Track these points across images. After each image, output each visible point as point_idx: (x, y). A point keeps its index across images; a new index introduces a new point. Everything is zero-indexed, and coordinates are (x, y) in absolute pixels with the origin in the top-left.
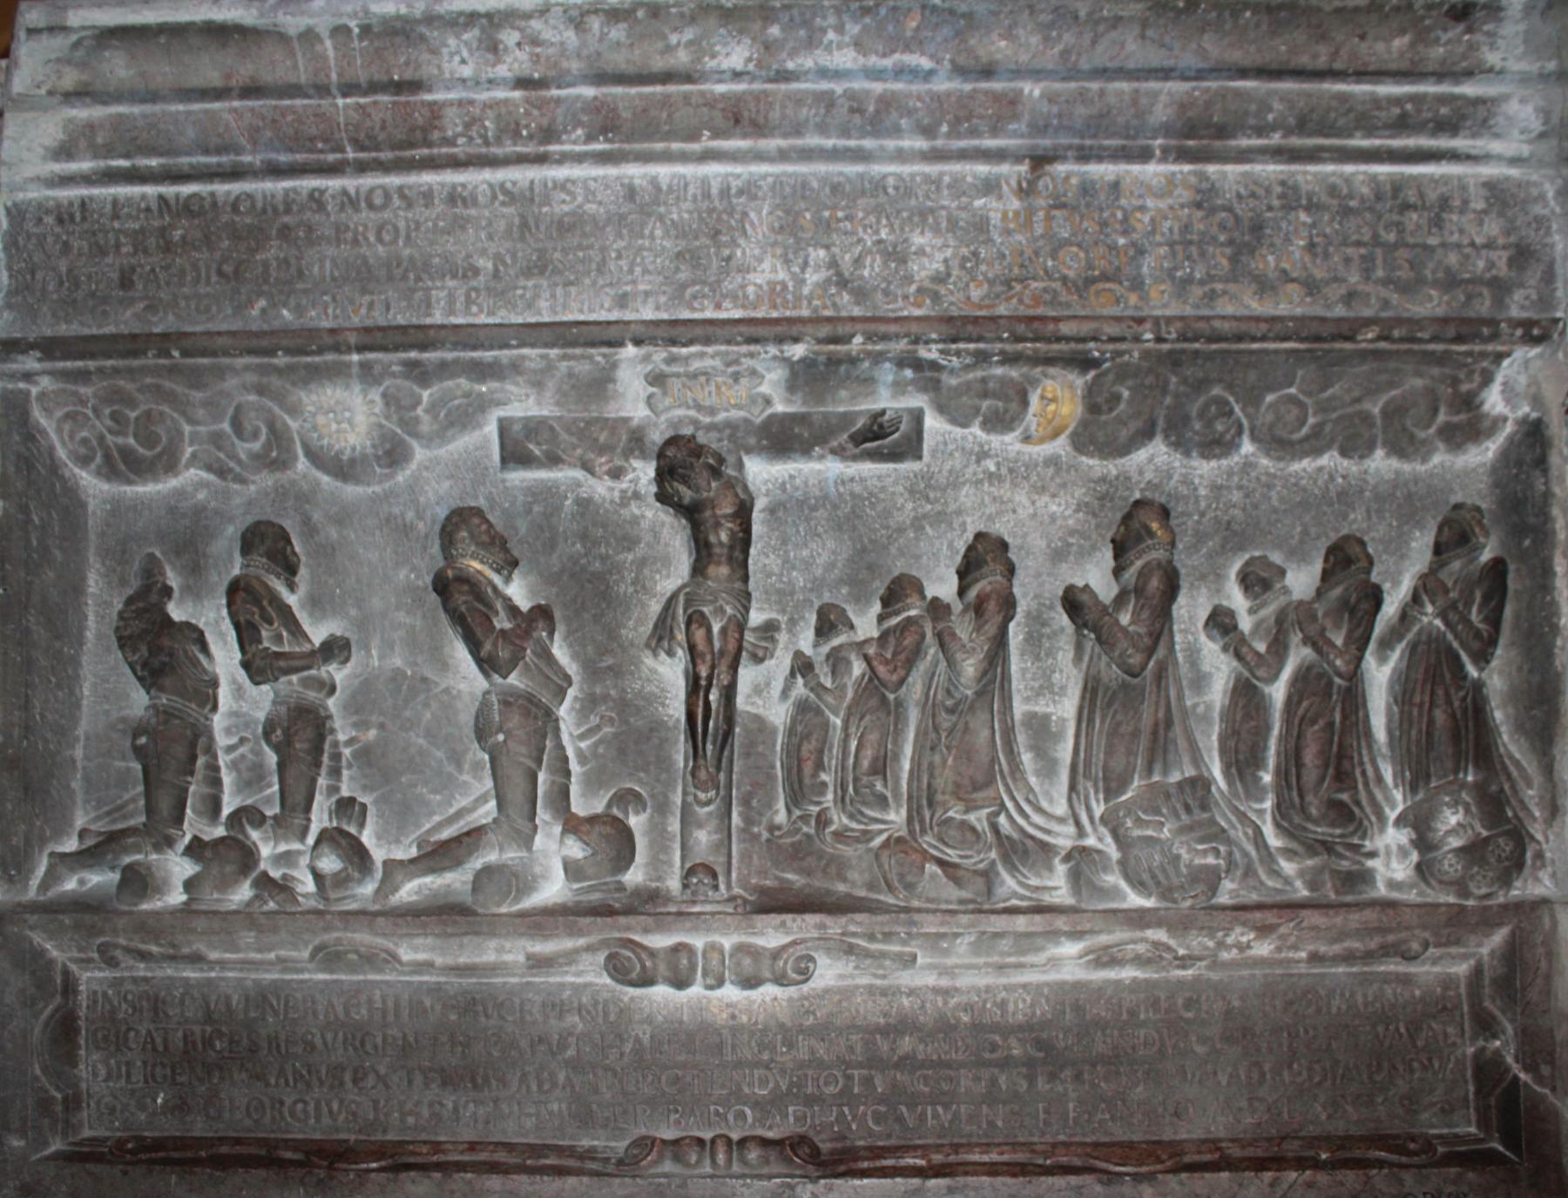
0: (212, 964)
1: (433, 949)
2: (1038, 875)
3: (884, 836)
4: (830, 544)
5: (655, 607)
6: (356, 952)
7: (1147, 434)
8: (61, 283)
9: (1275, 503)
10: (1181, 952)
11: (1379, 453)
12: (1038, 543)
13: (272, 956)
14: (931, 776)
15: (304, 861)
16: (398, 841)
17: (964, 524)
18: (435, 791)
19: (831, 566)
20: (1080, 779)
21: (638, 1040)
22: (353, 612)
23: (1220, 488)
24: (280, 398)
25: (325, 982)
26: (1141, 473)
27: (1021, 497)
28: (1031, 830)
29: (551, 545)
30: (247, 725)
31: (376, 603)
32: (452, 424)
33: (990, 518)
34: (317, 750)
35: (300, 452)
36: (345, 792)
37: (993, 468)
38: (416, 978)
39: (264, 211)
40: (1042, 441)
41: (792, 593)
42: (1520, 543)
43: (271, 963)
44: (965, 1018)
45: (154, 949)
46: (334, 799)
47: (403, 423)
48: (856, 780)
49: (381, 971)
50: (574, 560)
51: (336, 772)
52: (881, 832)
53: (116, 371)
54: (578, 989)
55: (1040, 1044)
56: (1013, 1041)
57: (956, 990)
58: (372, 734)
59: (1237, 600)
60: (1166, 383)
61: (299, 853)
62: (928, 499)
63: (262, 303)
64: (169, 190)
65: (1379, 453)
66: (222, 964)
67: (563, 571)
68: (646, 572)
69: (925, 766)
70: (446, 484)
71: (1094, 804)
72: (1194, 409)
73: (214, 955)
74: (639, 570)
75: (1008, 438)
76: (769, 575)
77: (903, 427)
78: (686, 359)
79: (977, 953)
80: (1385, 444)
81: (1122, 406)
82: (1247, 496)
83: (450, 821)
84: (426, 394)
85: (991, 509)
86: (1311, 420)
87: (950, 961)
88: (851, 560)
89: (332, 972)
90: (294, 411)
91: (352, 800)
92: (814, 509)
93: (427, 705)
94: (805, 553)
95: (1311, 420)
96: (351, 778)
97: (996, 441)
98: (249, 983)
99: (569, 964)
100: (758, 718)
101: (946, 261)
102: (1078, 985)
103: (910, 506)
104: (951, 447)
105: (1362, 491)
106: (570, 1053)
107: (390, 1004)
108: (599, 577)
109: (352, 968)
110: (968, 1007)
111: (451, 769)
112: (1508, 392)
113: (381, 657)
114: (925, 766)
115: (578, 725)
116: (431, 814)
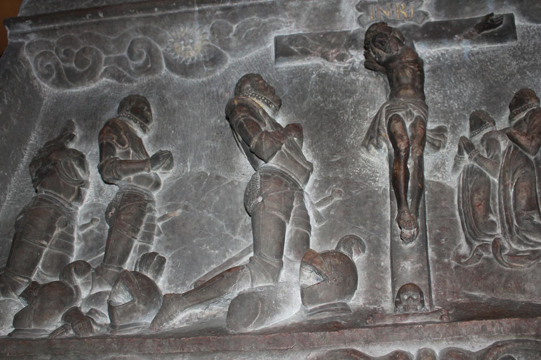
19: (473, 96)
22: (180, 142)
29: (303, 98)
50: (316, 104)
62: (524, 59)
68: (360, 107)
76: (436, 103)
77: (504, 22)
103: (515, 63)
104: (532, 34)
111: (228, 232)
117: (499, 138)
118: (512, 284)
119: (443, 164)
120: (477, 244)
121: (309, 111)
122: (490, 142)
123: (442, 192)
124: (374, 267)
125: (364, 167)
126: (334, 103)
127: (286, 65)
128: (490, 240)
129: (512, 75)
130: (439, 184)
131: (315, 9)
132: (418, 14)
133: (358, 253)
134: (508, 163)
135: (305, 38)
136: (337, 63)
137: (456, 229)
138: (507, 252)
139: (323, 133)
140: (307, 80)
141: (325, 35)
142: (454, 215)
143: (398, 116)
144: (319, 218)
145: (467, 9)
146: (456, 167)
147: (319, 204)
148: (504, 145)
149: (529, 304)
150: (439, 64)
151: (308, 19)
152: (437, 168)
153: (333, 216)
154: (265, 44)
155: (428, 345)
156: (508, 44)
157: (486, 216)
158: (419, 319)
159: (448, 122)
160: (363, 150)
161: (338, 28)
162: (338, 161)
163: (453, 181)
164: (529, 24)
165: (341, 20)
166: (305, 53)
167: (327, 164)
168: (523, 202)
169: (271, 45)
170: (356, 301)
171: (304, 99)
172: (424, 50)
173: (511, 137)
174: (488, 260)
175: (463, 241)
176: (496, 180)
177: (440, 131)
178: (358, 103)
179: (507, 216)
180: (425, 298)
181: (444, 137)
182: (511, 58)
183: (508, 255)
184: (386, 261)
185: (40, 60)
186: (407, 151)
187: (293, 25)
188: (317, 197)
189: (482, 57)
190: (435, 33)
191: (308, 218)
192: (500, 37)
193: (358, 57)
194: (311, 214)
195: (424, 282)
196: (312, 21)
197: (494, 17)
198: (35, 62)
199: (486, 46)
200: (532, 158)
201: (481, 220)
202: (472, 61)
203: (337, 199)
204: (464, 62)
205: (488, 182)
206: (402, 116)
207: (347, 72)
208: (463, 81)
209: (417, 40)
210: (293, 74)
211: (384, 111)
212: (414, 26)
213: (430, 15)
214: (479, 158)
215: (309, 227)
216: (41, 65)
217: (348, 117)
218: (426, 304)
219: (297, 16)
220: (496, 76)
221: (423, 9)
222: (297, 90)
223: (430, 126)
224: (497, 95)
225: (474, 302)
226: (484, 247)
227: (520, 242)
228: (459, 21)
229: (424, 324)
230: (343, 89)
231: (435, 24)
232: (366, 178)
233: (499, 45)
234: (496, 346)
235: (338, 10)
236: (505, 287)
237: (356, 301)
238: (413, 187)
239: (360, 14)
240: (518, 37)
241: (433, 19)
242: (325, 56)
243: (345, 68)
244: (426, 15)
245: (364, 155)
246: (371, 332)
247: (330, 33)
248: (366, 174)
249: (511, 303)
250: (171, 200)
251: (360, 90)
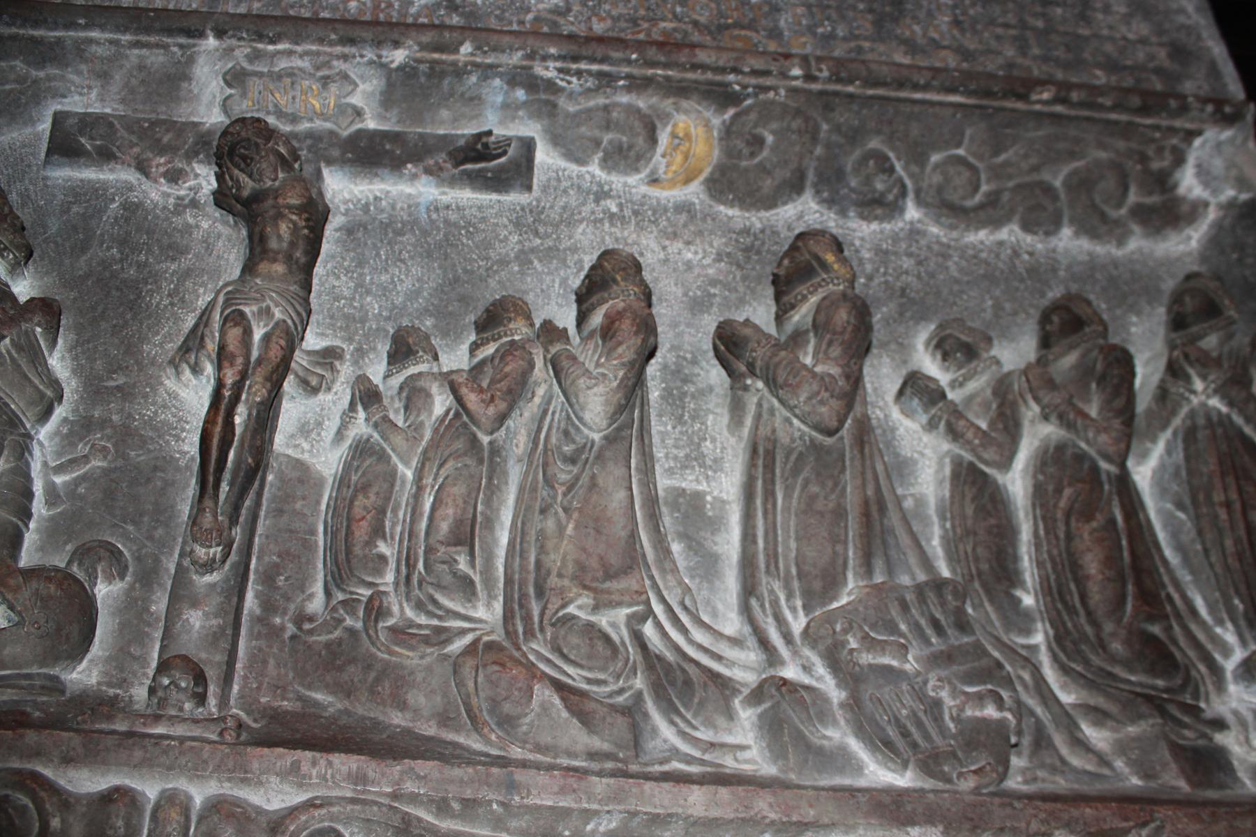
4: (416, 271)
9: (956, 274)
17: (581, 261)
19: (414, 294)
23: (886, 252)
41: (363, 321)
69: (532, 537)
76: (337, 299)
82: (920, 263)
88: (440, 290)
94: (384, 278)
117: (435, 389)
118: (386, 688)
119: (319, 424)
120: (340, 596)
121: (87, 276)
122: (414, 395)
123: (301, 481)
125: (165, 406)
127: (65, 174)
128: (366, 592)
130: (300, 465)
131: (141, 67)
132: (342, 109)
133: (109, 579)
134: (434, 444)
135: (111, 125)
136: (165, 187)
137: (310, 562)
138: (391, 622)
139: (104, 325)
141: (153, 124)
142: (313, 532)
143: (242, 314)
144: (52, 496)
146: (340, 435)
147: (59, 469)
148: (441, 403)
149: (408, 732)
150: (365, 218)
151: (126, 85)
152: (304, 430)
153: (82, 498)
154: (32, 122)
155: (181, 784)
156: (515, 198)
157: (370, 543)
158: (179, 730)
159: (350, 340)
160: (170, 371)
161: (182, 113)
162: (118, 388)
163: (328, 461)
164: (563, 163)
165: (193, 99)
166: (106, 156)
167: (94, 390)
168: (444, 527)
169: (45, 126)
170: (84, 675)
172: (341, 187)
173: (454, 389)
174: (352, 632)
175: (318, 588)
176: (409, 474)
177: (329, 356)
178: (188, 273)
179: (409, 549)
180: (212, 689)
181: (332, 368)
182: (511, 227)
183: (393, 630)
184: (160, 605)
186: (238, 387)
187: (94, 95)
188: (59, 454)
189: (453, 217)
190: (369, 154)
191: (29, 495)
192: (498, 182)
193: (204, 178)
194: (38, 488)
195: (220, 657)
196: (132, 91)
197: (493, 139)
199: (466, 196)
200: (485, 439)
201: (357, 550)
203: (97, 463)
204: (416, 222)
205: (392, 475)
206: (249, 315)
207: (180, 206)
208: (403, 261)
209: (330, 162)
210: (76, 195)
211: (221, 299)
212: (332, 133)
213: (368, 115)
214: (384, 425)
215: (26, 515)
218: (212, 702)
219: (104, 77)
220: (472, 260)
221: (356, 100)
222: (75, 228)
223: (313, 341)
224: (463, 299)
225: (310, 712)
226: (350, 605)
227: (419, 606)
228: (421, 136)
229: (182, 740)
231: (375, 133)
232: (162, 430)
233: (494, 197)
234: (310, 805)
235: (188, 78)
236: (372, 691)
237: (84, 675)
238: (238, 462)
239: (229, 91)
240: (535, 187)
242: (142, 168)
243: (179, 198)
244: (358, 113)
245: (170, 383)
246: (76, 740)
247: (164, 122)
248: (164, 423)
249: (376, 724)
251: (198, 248)
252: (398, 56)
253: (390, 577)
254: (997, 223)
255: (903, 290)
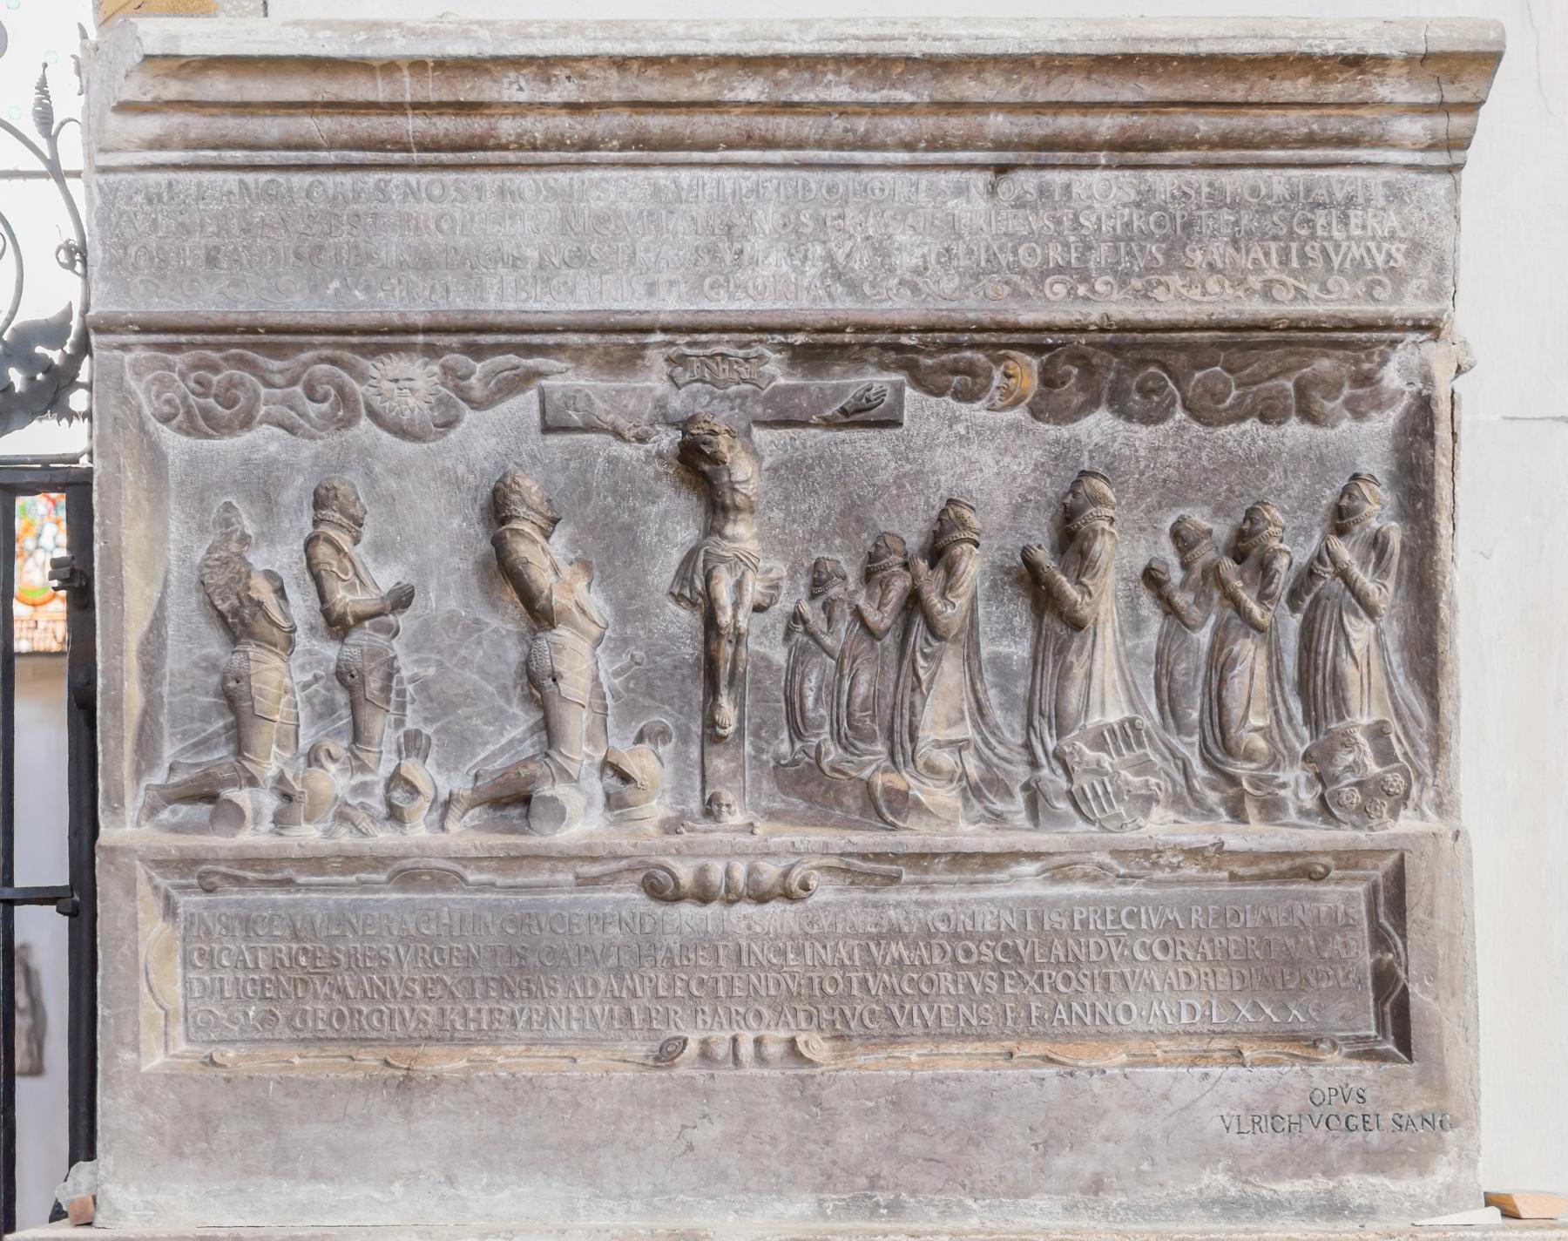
0: (299, 887)
1: (496, 870)
2: (1002, 800)
3: (874, 767)
4: (826, 499)
5: (676, 556)
6: (430, 874)
7: (1091, 405)
8: (152, 259)
10: (1122, 871)
11: (1294, 420)
12: (1001, 500)
13: (352, 879)
14: (913, 714)
15: (379, 790)
16: (456, 769)
18: (487, 723)
19: (824, 520)
20: (1036, 715)
21: (669, 950)
22: (412, 558)
24: (349, 368)
25: (399, 900)
26: (1089, 436)
27: (987, 457)
28: (995, 760)
29: (587, 497)
30: (319, 663)
31: (433, 550)
32: (500, 390)
33: (961, 477)
34: (386, 689)
35: (363, 411)
36: (410, 725)
37: (963, 432)
38: (479, 896)
39: (335, 198)
40: (1003, 409)
42: (1414, 505)
43: (352, 885)
44: (943, 928)
45: (250, 875)
46: (401, 732)
47: (458, 390)
48: (849, 715)
49: (447, 889)
50: (606, 511)
51: (402, 706)
52: (871, 763)
53: (206, 345)
54: (618, 903)
55: (1005, 947)
56: (984, 949)
57: (936, 903)
58: (432, 671)
59: (1168, 553)
60: (1110, 362)
61: (374, 783)
63: (336, 284)
64: (249, 177)
65: (1294, 420)
66: (308, 887)
67: (596, 521)
70: (493, 441)
71: (1047, 739)
72: (1133, 384)
73: (302, 879)
74: (662, 522)
75: (977, 405)
77: (886, 399)
78: (705, 345)
79: (951, 871)
80: (1298, 413)
81: (1073, 381)
82: (1180, 457)
83: (503, 750)
84: (479, 366)
85: (961, 469)
86: (1234, 393)
87: (929, 878)
88: (842, 513)
89: (405, 891)
90: (362, 377)
91: (418, 733)
92: (810, 468)
93: (479, 643)
94: (804, 507)
95: (1234, 393)
96: (414, 711)
97: (964, 409)
98: (330, 903)
99: (612, 882)
100: (764, 658)
101: (924, 256)
102: (1036, 900)
105: (1279, 454)
106: (612, 962)
107: (456, 918)
108: (627, 529)
109: (425, 888)
110: (946, 918)
111: (501, 702)
112: (1404, 369)
113: (438, 599)
114: (907, 705)
115: (612, 663)
116: (485, 744)
124: (681, 756)
126: (632, 510)
129: (886, 487)
140: (592, 465)
145: (837, 368)
152: (764, 631)
153: (633, 691)
171: (588, 500)
175: (785, 735)
181: (777, 587)
185: (155, 388)
198: (147, 391)
202: (833, 456)
208: (816, 492)
216: (158, 397)
217: (649, 538)
230: (645, 488)
241: (782, 381)
250: (417, 651)
252: (799, 339)
253: (827, 728)
254: (1242, 418)
255: (1165, 481)
